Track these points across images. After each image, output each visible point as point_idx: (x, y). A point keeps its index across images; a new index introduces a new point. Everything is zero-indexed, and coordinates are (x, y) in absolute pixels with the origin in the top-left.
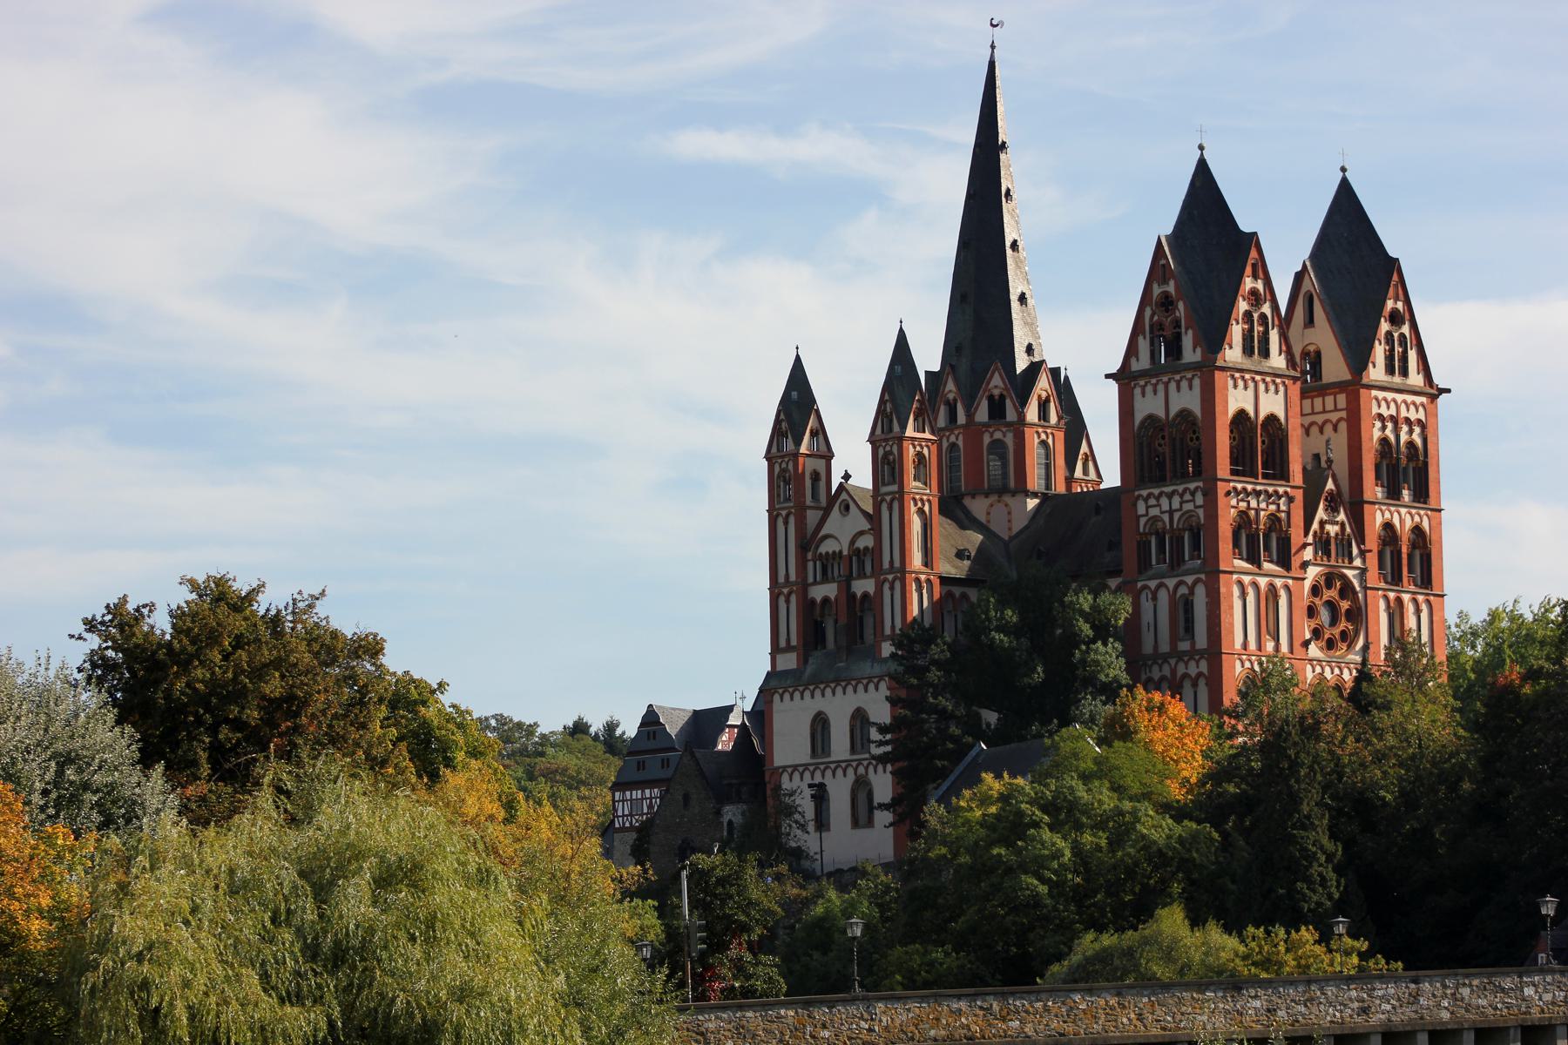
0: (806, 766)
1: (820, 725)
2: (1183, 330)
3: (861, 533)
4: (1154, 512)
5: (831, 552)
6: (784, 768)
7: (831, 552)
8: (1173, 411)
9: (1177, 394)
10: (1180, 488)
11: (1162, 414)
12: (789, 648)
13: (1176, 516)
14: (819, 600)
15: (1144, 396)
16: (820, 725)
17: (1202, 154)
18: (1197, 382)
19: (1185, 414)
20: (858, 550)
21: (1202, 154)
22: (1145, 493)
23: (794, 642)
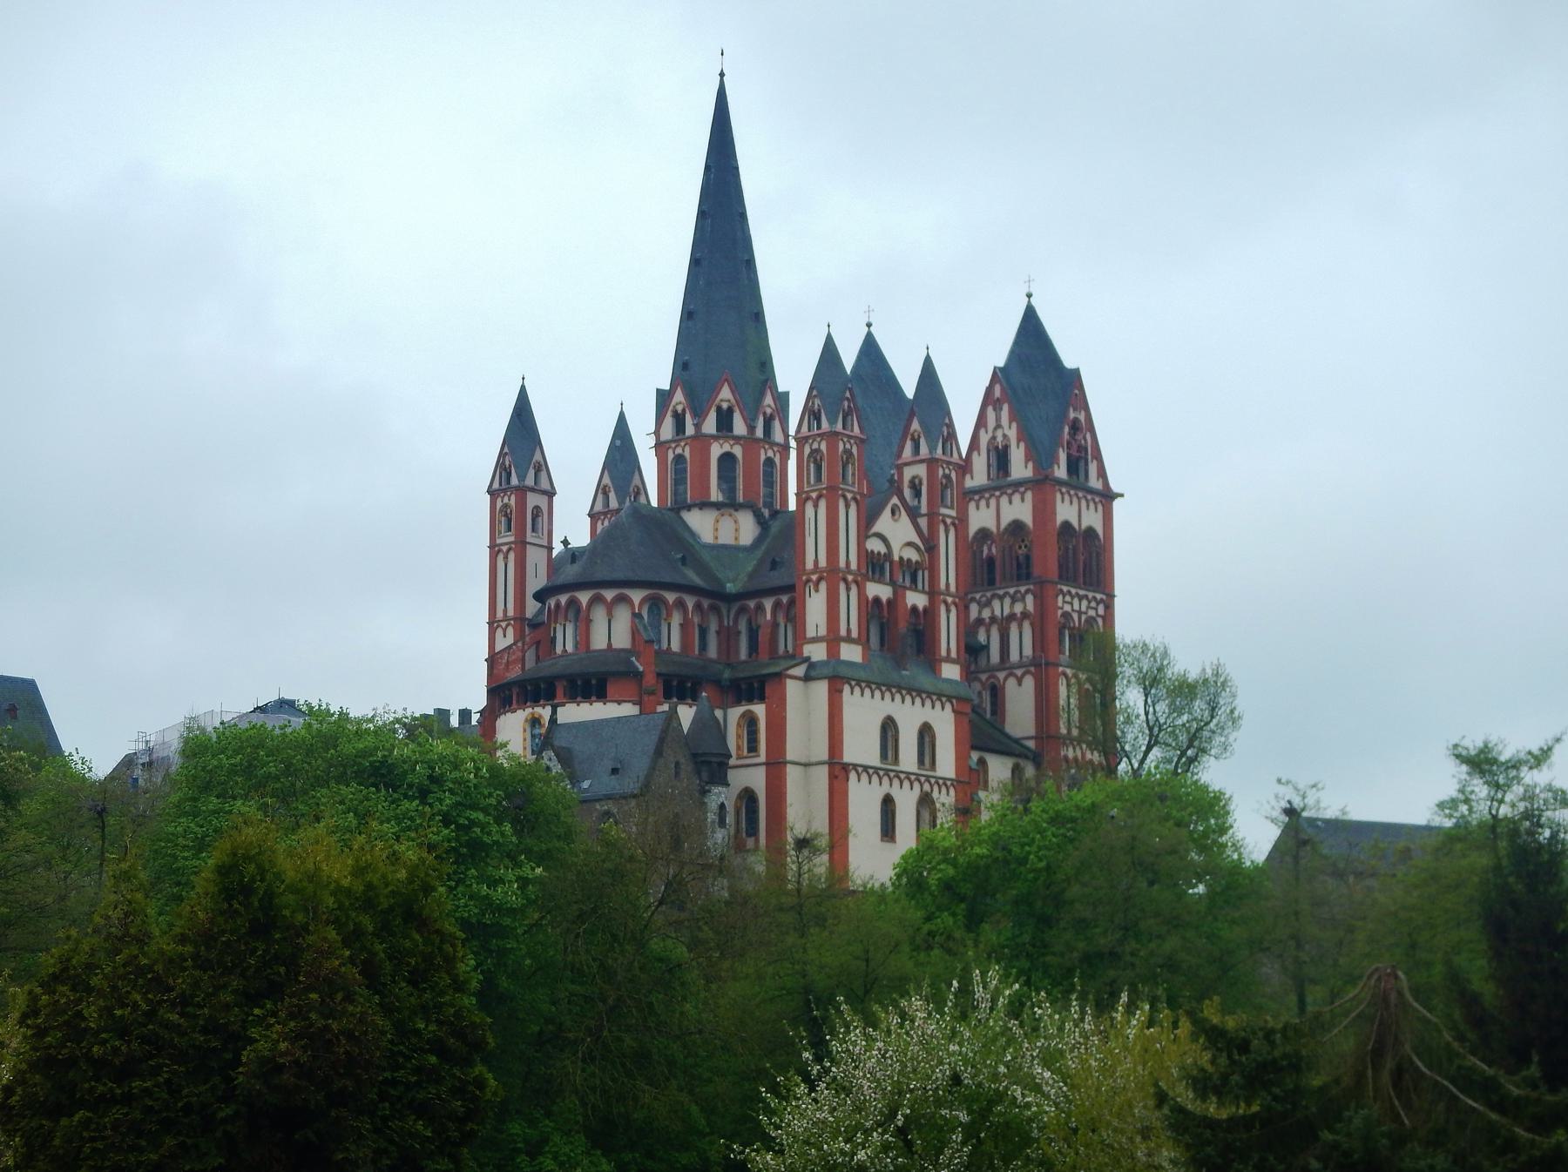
0: (876, 770)
1: (889, 728)
2: (1090, 457)
3: (909, 544)
4: (1067, 608)
5: (876, 552)
6: (855, 766)
7: (876, 552)
8: (1084, 526)
9: (1086, 511)
10: (1090, 595)
11: (1075, 524)
12: (849, 639)
13: (1083, 617)
14: (870, 597)
15: (1063, 502)
16: (889, 728)
17: (1029, 301)
18: (1100, 507)
19: (1090, 531)
20: (901, 558)
21: (1029, 301)
22: (1065, 589)
23: (855, 634)
